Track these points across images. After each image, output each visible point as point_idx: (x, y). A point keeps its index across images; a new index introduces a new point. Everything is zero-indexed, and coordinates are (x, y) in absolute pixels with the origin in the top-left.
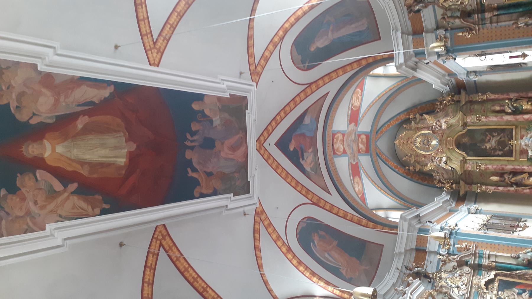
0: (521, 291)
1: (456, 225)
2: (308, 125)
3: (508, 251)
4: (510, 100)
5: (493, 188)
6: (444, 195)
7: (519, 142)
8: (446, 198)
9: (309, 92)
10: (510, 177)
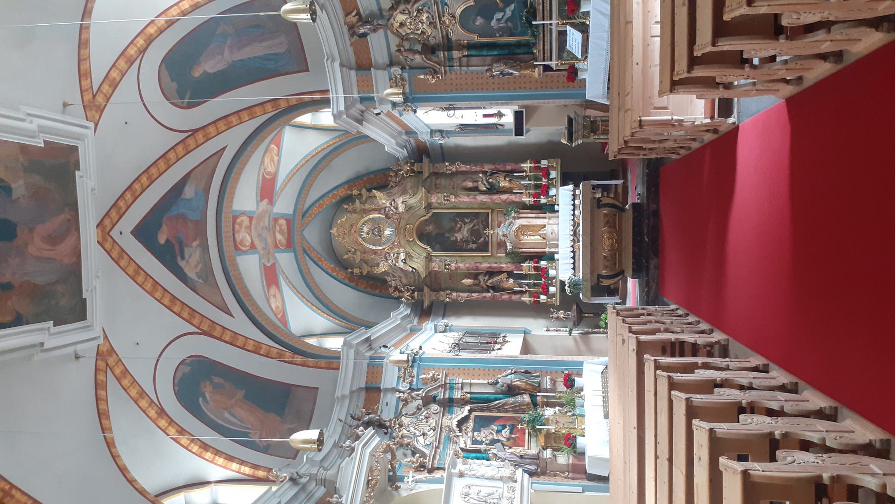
0: (500, 428)
1: (421, 348)
2: (190, 200)
3: (485, 376)
4: (485, 173)
5: (465, 295)
6: (402, 308)
8: (406, 313)
9: (193, 146)
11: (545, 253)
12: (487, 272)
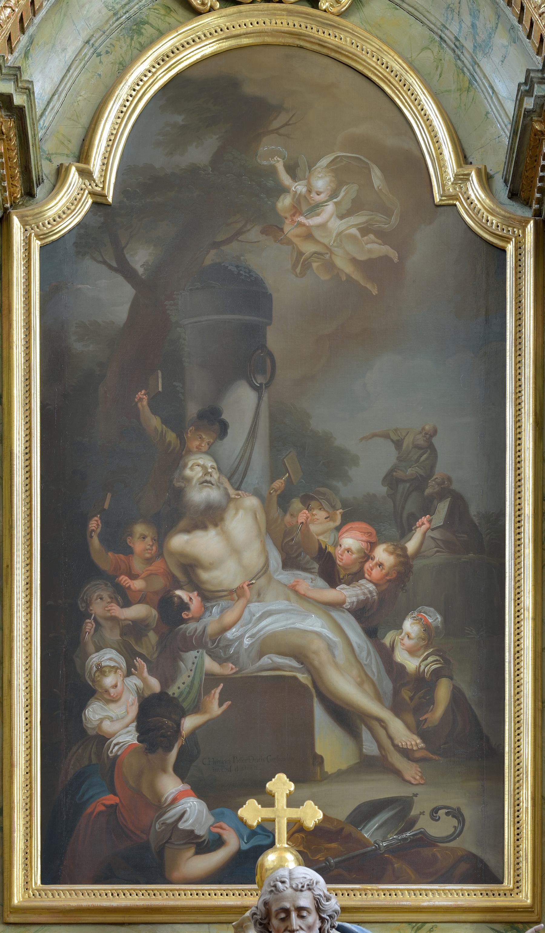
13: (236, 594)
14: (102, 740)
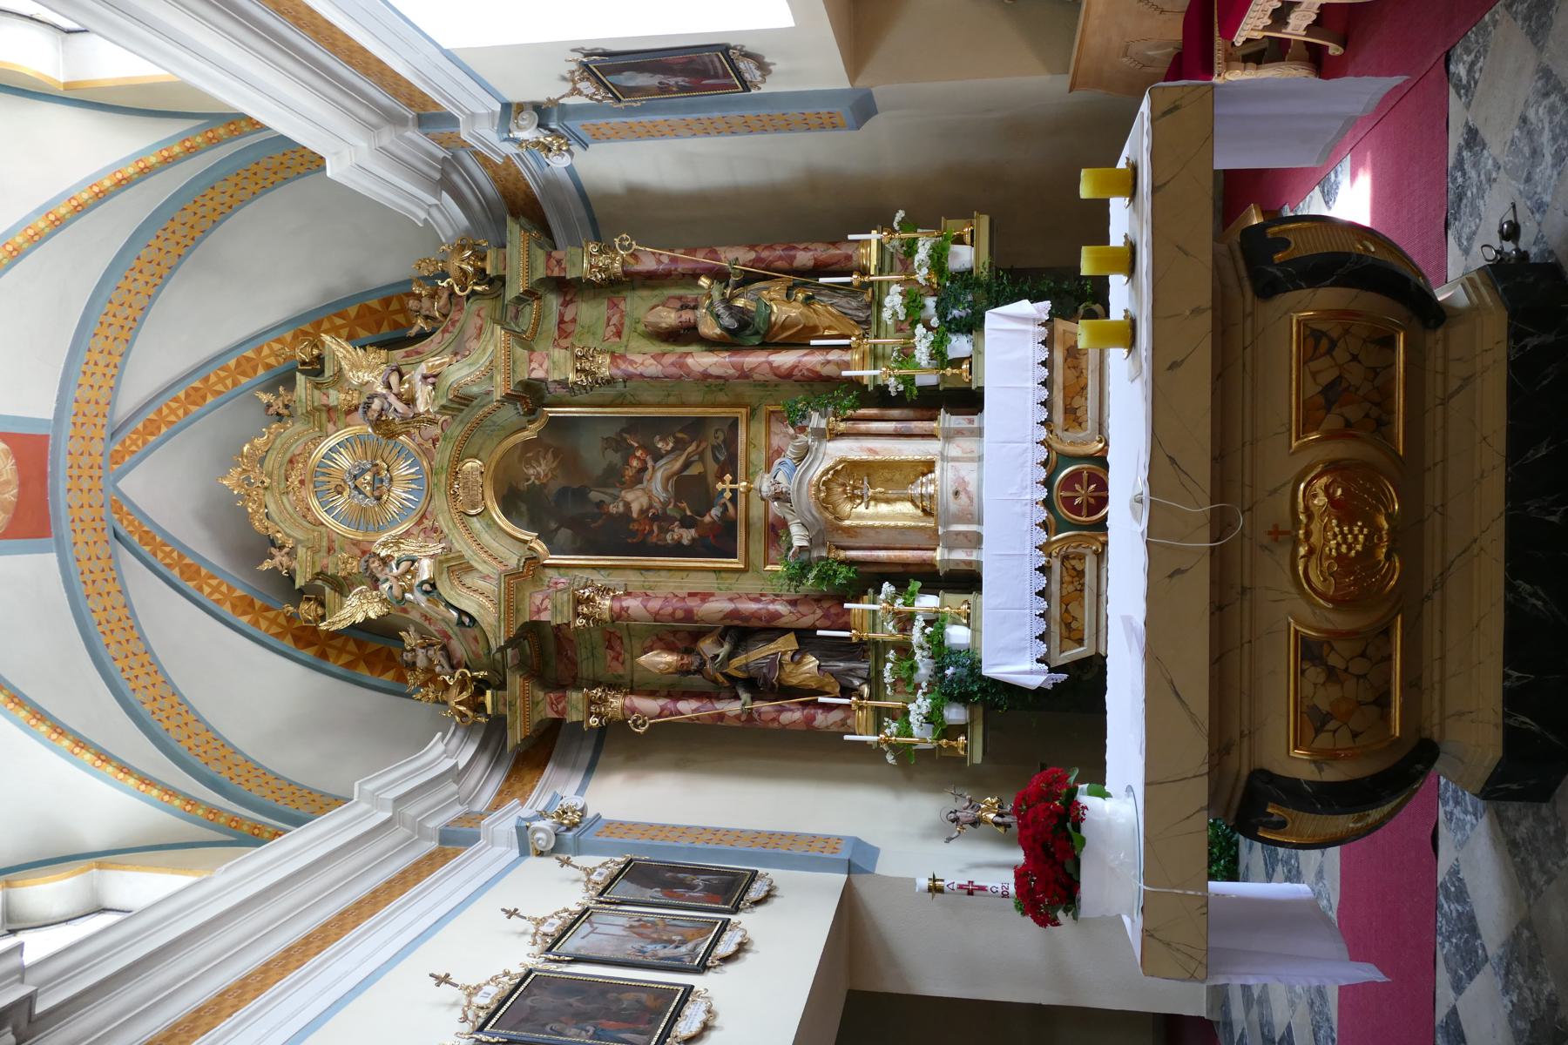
4: (719, 275)
5: (649, 705)
7: (756, 485)
10: (722, 652)
11: (931, 564)
12: (727, 629)
13: (650, 498)
14: (693, 539)
